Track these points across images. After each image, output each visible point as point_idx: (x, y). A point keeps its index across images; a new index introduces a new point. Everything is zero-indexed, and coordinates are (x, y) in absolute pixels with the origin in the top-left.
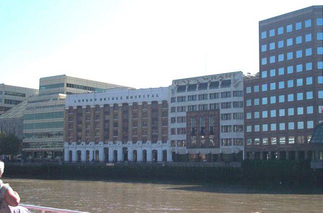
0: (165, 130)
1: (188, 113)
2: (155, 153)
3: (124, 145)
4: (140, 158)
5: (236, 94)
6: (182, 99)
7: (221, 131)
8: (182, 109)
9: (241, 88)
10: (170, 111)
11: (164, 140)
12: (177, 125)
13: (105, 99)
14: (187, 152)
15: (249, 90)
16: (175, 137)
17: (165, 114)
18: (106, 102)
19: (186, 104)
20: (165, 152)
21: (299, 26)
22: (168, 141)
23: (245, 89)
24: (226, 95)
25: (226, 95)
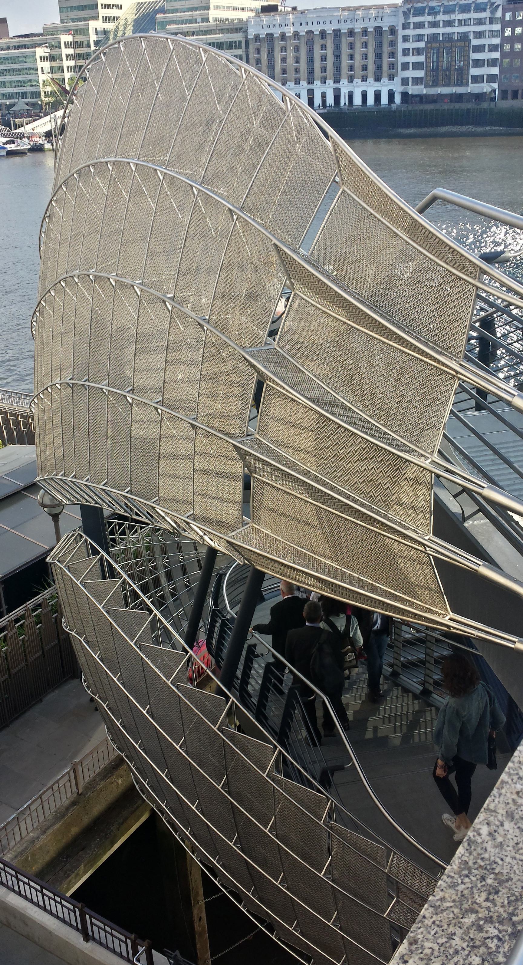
0: (392, 66)
1: (427, 43)
2: (378, 96)
4: (357, 101)
6: (420, 25)
7: (470, 67)
8: (419, 38)
9: (499, 14)
10: (400, 40)
11: (391, 78)
12: (412, 59)
13: (307, 24)
14: (425, 93)
15: (508, 16)
16: (411, 74)
17: (393, 43)
18: (309, 28)
19: (426, 31)
20: (391, 95)
22: (395, 78)
23: (504, 15)
24: (480, 22)
25: (480, 22)
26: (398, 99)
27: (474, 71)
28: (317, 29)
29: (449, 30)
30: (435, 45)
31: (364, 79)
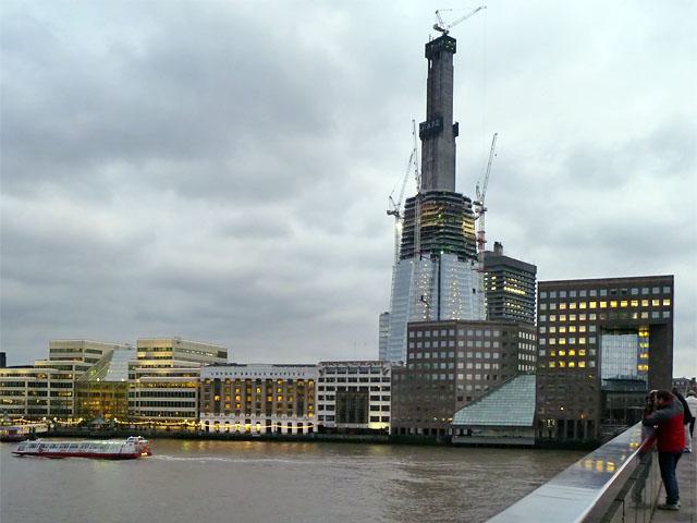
3: (268, 418)
5: (385, 380)
6: (332, 380)
8: (329, 389)
9: (389, 375)
10: (317, 388)
12: (326, 403)
15: (396, 377)
16: (325, 413)
18: (248, 376)
19: (336, 384)
21: (444, 333)
24: (377, 380)
25: (377, 380)
26: (315, 430)
27: (372, 414)
28: (254, 378)
29: (352, 384)
30: (343, 394)
31: (290, 414)
